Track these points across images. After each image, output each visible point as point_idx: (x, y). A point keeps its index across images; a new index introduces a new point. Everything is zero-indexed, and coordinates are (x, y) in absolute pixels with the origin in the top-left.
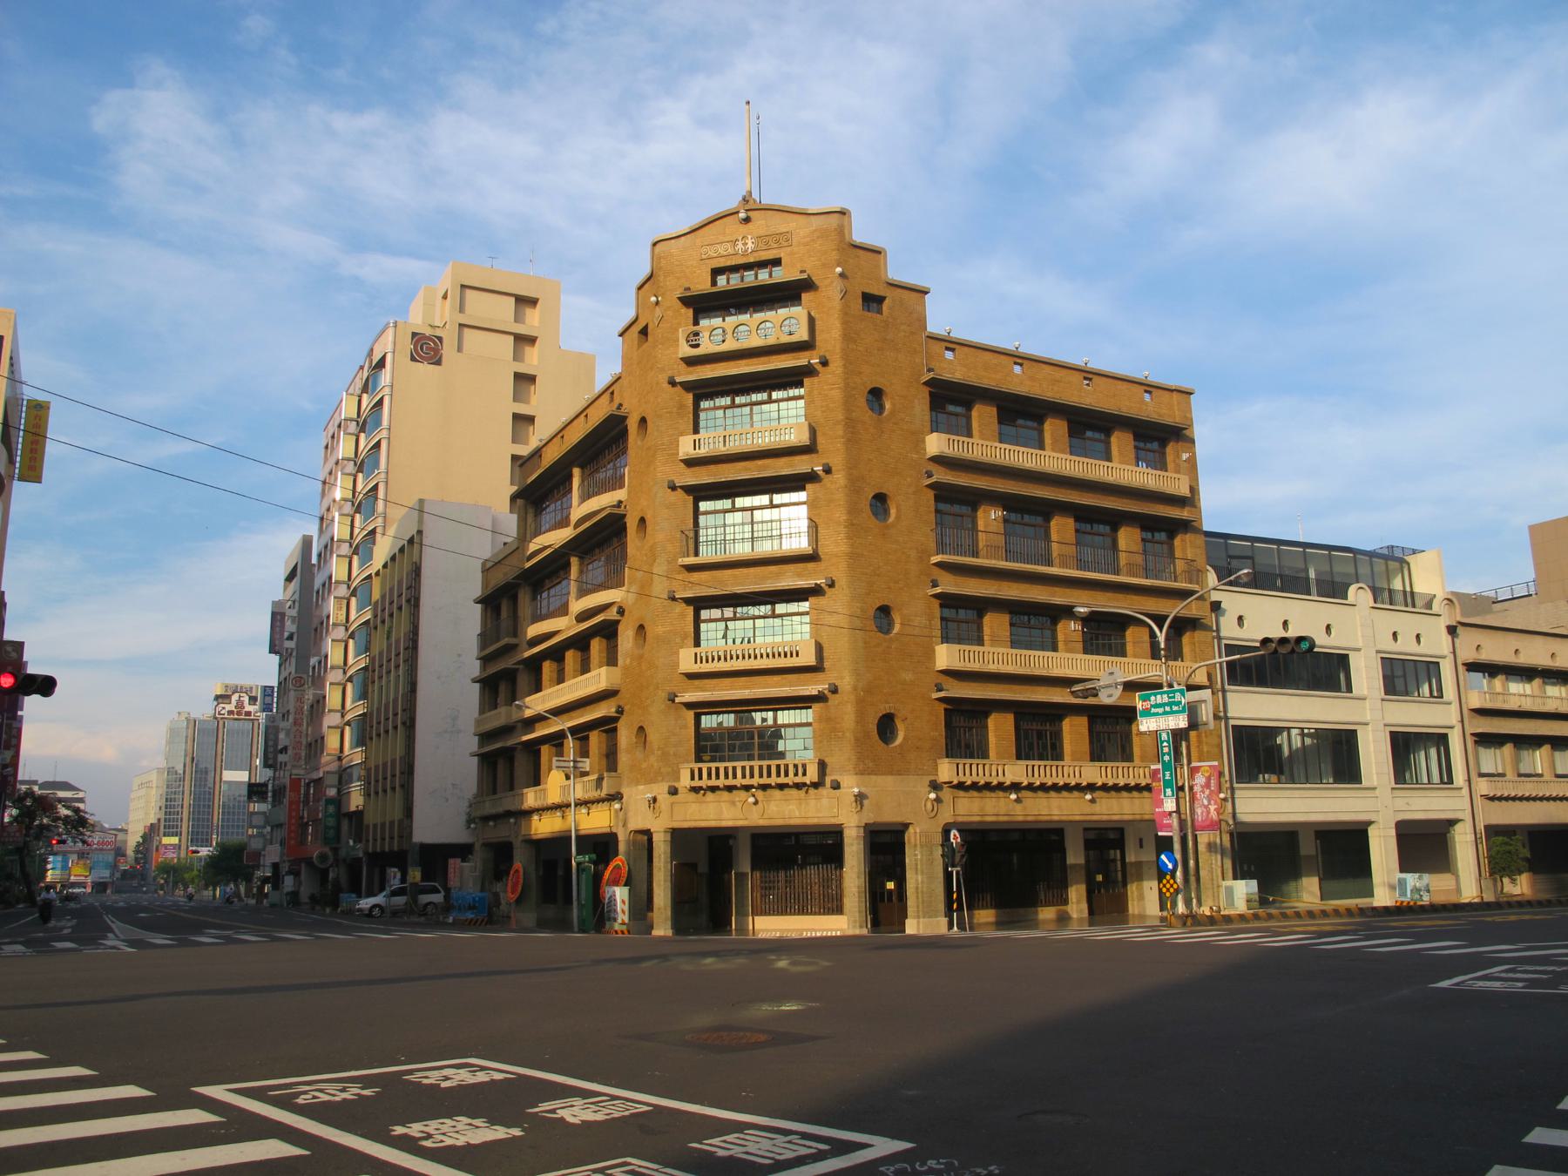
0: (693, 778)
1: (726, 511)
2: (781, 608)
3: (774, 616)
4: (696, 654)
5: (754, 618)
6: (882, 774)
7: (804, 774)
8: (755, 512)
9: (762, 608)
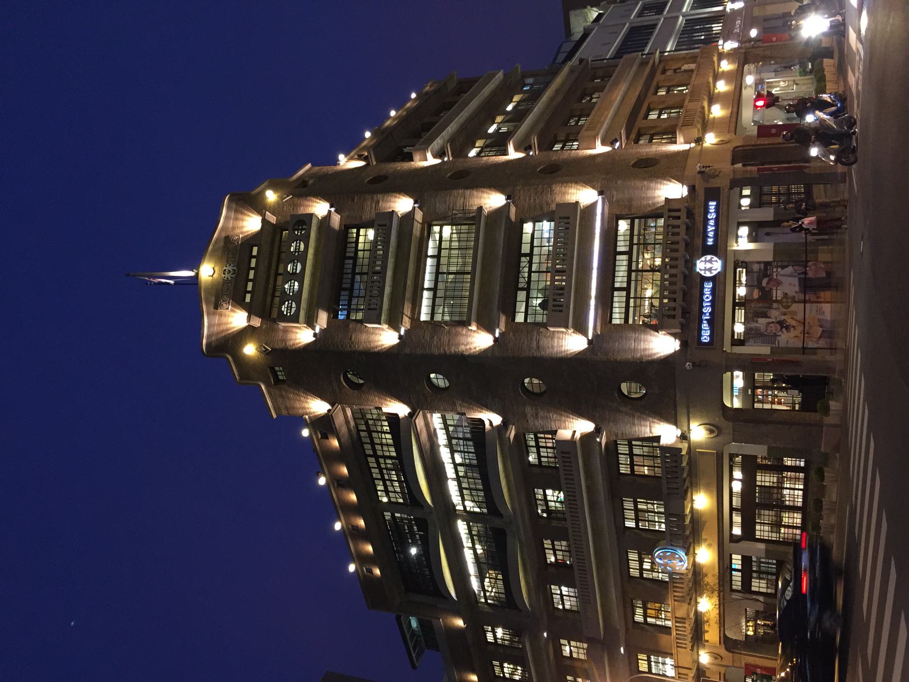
0: (674, 317)
1: (434, 298)
2: (525, 249)
3: (531, 255)
5: (530, 272)
6: (686, 164)
7: (679, 210)
9: (522, 265)
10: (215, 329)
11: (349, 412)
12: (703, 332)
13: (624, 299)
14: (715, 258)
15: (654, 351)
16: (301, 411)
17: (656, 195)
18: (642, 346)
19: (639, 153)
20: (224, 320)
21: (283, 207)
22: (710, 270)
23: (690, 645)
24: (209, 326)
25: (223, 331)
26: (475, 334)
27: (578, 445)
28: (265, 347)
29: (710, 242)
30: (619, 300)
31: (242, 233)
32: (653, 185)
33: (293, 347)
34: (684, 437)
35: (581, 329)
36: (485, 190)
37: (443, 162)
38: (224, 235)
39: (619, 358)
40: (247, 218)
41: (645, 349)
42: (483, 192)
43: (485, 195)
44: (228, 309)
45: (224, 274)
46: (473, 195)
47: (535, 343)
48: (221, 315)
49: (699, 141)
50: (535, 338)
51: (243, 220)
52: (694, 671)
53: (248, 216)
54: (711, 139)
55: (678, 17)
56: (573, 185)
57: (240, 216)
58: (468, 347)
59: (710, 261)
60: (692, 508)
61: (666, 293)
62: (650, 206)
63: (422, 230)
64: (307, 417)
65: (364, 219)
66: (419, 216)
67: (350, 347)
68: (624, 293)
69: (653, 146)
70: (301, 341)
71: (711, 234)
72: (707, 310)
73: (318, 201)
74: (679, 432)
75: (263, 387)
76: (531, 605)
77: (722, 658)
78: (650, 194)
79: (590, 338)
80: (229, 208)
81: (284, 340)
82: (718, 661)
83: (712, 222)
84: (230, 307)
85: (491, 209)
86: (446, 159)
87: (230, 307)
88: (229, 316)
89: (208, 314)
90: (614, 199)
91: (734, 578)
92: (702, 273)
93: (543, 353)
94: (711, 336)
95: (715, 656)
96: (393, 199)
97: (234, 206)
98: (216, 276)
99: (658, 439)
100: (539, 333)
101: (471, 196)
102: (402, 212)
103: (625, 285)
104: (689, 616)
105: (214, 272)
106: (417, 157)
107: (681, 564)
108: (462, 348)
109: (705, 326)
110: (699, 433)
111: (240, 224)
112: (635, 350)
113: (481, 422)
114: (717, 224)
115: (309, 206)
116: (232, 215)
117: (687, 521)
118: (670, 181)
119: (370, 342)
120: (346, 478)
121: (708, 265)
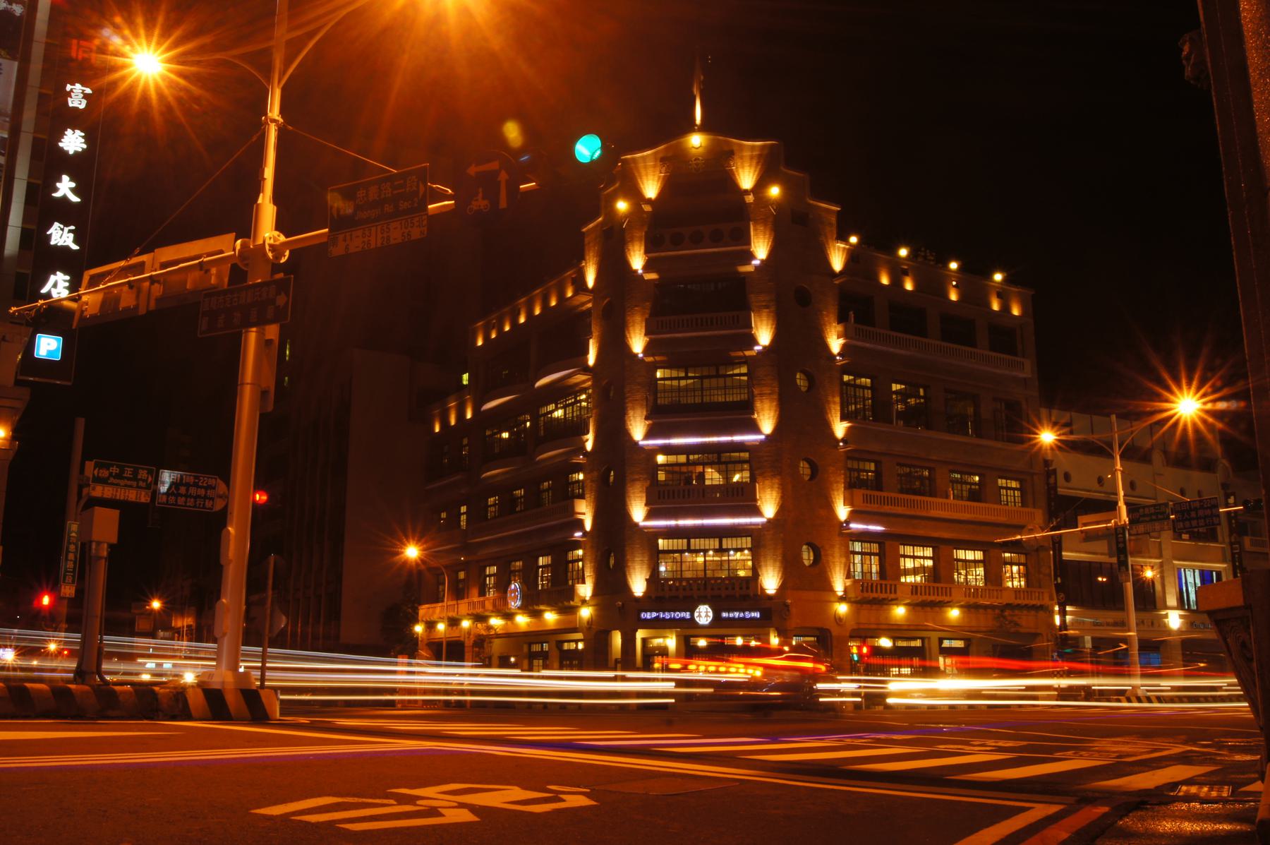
4: (659, 492)
7: (748, 588)
8: (704, 380)
10: (641, 165)
11: (590, 305)
12: (649, 613)
13: (680, 548)
14: (710, 619)
15: (633, 576)
16: (587, 258)
17: (769, 568)
18: (638, 567)
19: (832, 546)
20: (650, 171)
21: (763, 208)
22: (700, 616)
23: (470, 612)
24: (644, 158)
25: (639, 173)
26: (643, 424)
27: (571, 519)
28: (625, 222)
29: (725, 615)
30: (680, 543)
31: (737, 168)
32: (778, 564)
33: (626, 250)
34: (584, 602)
35: (650, 516)
36: (777, 413)
37: (832, 357)
38: (735, 148)
39: (627, 548)
40: (752, 170)
41: (634, 569)
42: (776, 411)
43: (772, 414)
44: (661, 173)
45: (696, 160)
46: (773, 402)
47: (637, 477)
48: (655, 166)
49: (842, 599)
50: (641, 476)
51: (750, 166)
52: (457, 617)
53: (755, 171)
54: (842, 609)
55: (1160, 556)
56: (780, 495)
57: (755, 162)
58: (632, 418)
59: (707, 616)
60: (545, 611)
61: (684, 584)
62: (759, 563)
63: (740, 357)
64: (583, 264)
65: (752, 295)
66: (748, 353)
67: (629, 307)
68: (685, 548)
69: (843, 560)
70: (633, 258)
71: (731, 615)
72: (667, 615)
73: (770, 243)
74: (587, 598)
75: (600, 219)
76: (485, 478)
77: (469, 638)
78: (770, 562)
79: (642, 524)
80: (763, 147)
81: (632, 240)
82: (467, 636)
83: (742, 615)
84: (663, 175)
85: (759, 421)
86: (838, 358)
87: (663, 175)
88: (654, 175)
89: (655, 154)
90: (766, 533)
91: (537, 645)
92: (697, 610)
93: (629, 485)
94: (646, 620)
95: (469, 632)
96: (770, 322)
97: (766, 152)
98: (694, 150)
99: (584, 582)
100: (645, 479)
101: (772, 400)
102: (757, 334)
103: (692, 548)
104: (486, 611)
105: (697, 148)
106: (840, 328)
107: (514, 604)
108: (631, 413)
109: (654, 615)
110: (586, 613)
111: (747, 164)
112: (633, 561)
113: (588, 433)
114: (739, 618)
115: (765, 233)
116: (756, 153)
117: (536, 607)
118: (781, 579)
119: (633, 326)
120: (534, 313)
121: (703, 614)
